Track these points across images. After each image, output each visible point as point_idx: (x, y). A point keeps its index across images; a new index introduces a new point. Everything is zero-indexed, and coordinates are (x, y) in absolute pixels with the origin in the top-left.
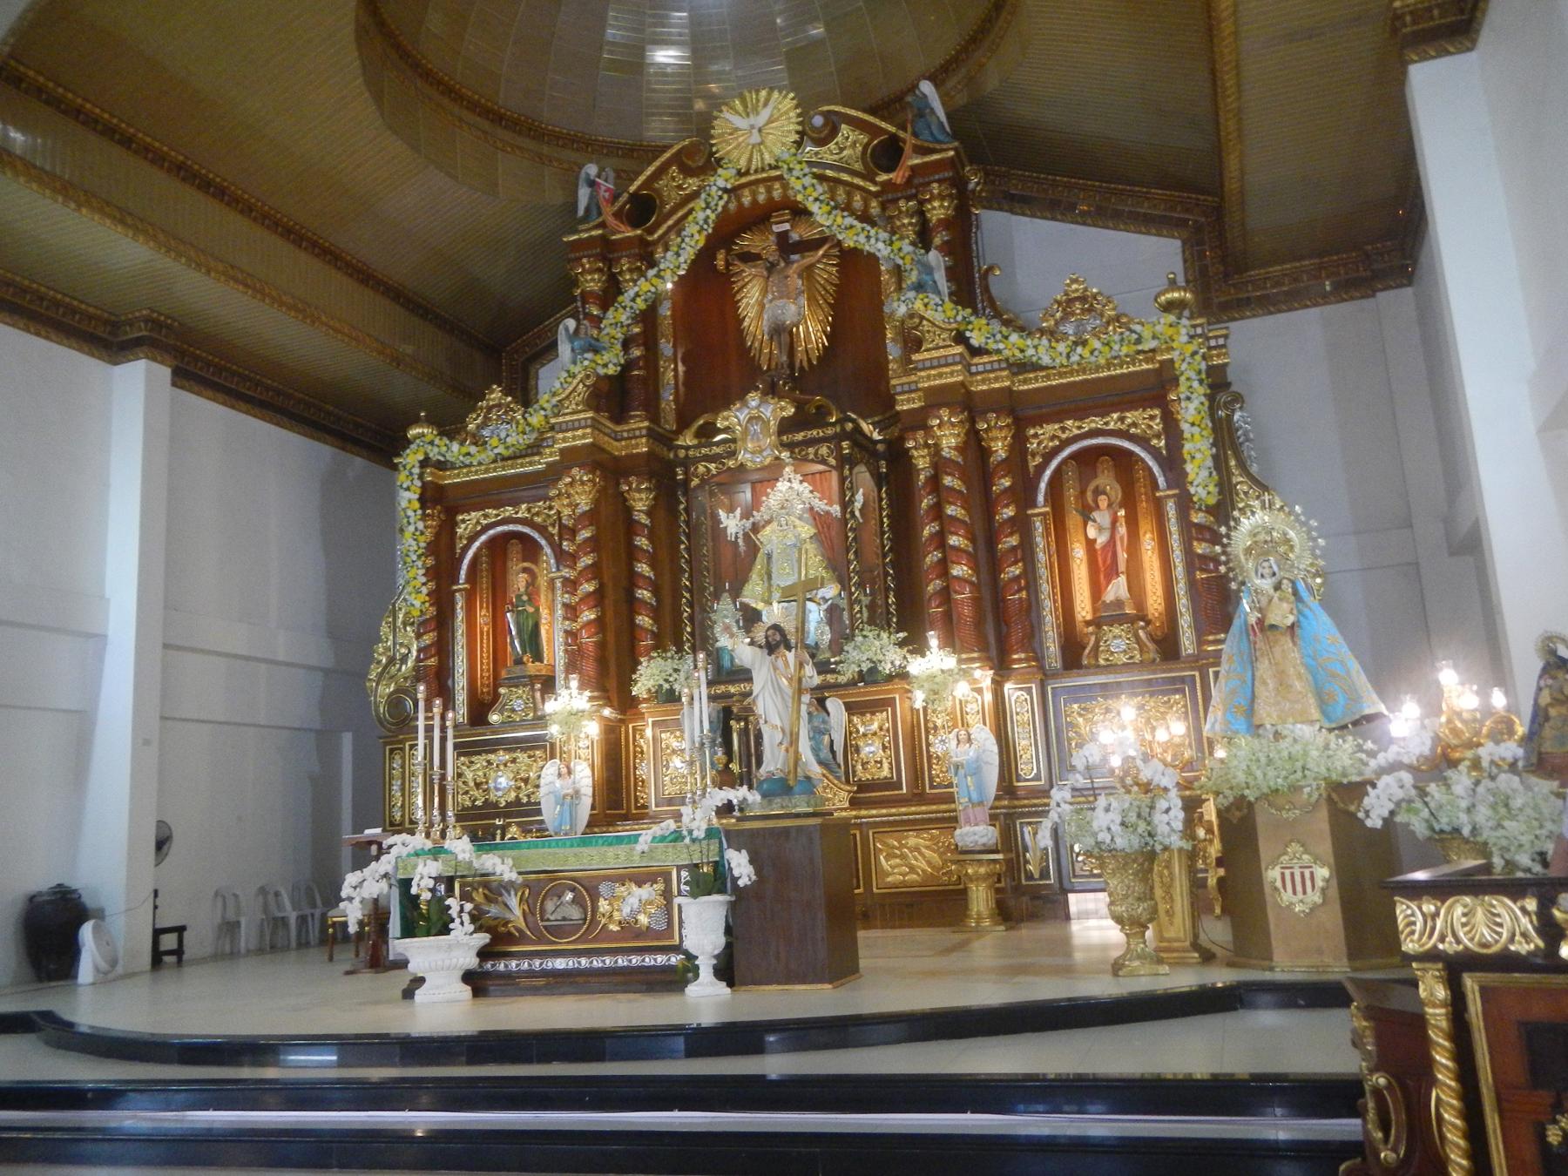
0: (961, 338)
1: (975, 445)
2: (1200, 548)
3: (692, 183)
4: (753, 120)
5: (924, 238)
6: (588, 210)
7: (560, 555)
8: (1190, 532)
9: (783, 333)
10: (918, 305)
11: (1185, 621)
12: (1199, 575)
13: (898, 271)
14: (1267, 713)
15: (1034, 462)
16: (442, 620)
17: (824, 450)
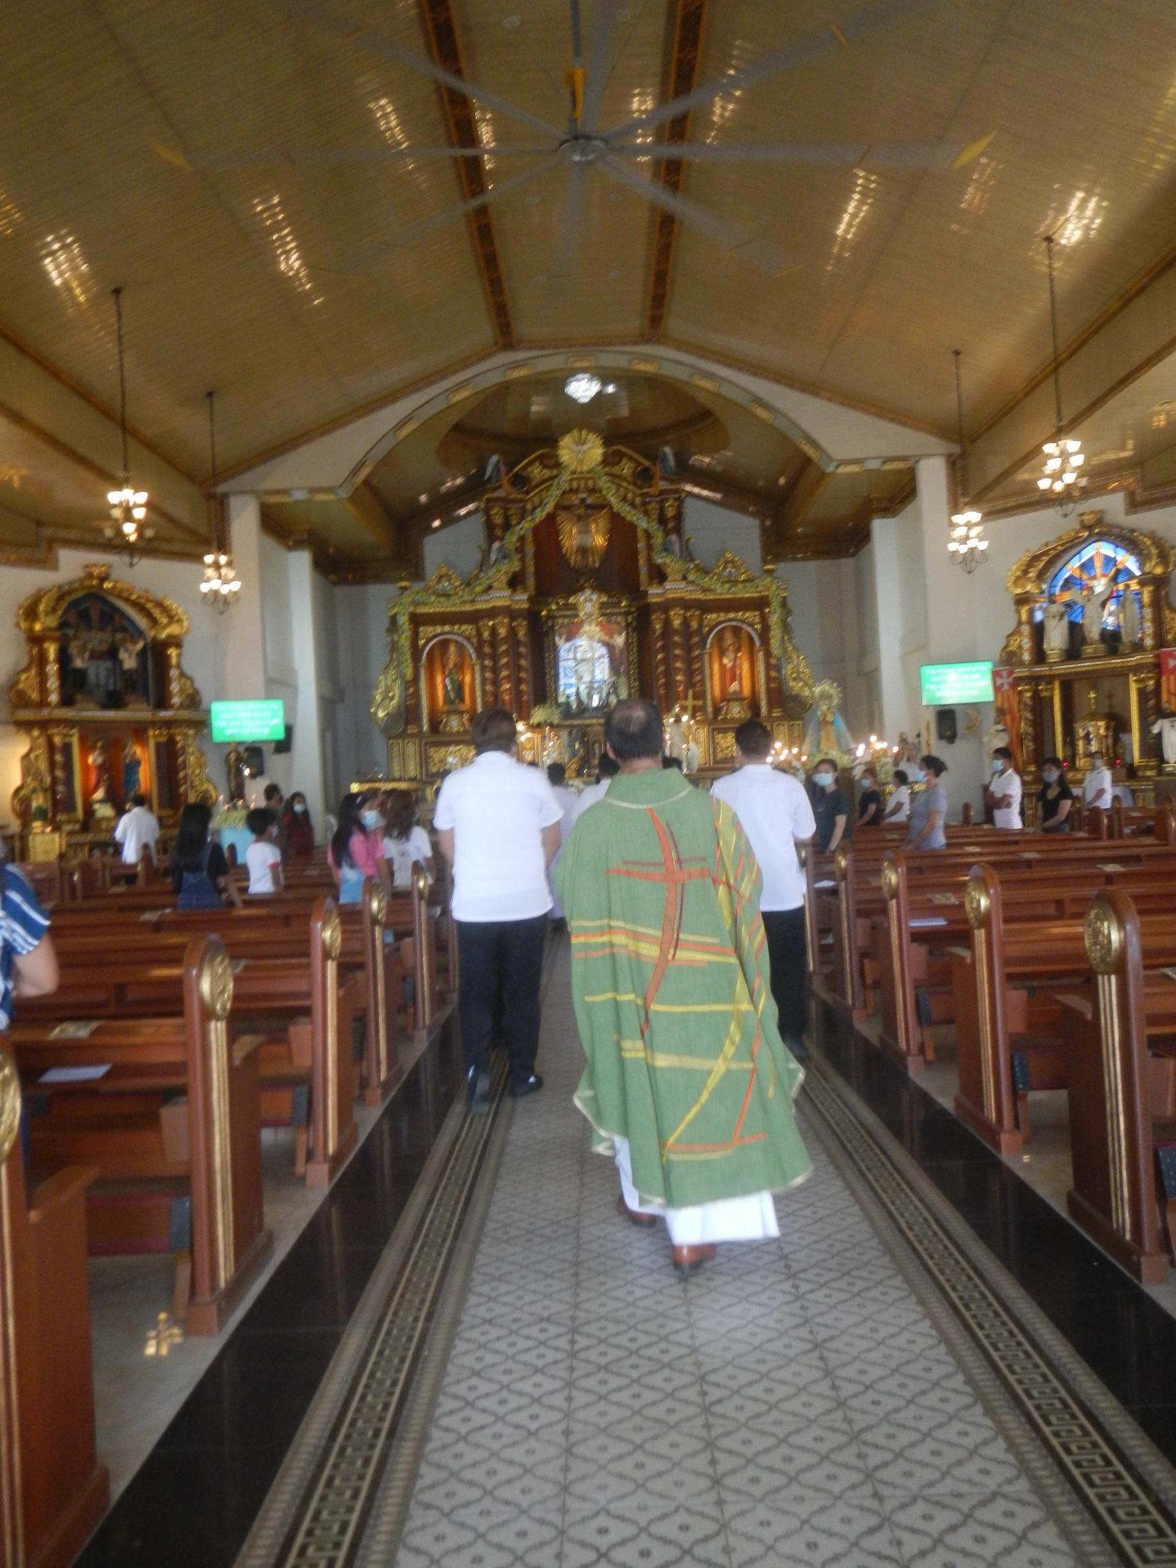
0: (684, 578)
1: (686, 623)
2: (773, 674)
3: (547, 473)
4: (579, 448)
5: (662, 520)
6: (490, 477)
7: (481, 656)
8: (768, 667)
9: (583, 550)
10: (668, 560)
11: (763, 704)
12: (773, 685)
13: (648, 535)
14: (823, 747)
15: (706, 630)
16: (416, 679)
17: (619, 619)
